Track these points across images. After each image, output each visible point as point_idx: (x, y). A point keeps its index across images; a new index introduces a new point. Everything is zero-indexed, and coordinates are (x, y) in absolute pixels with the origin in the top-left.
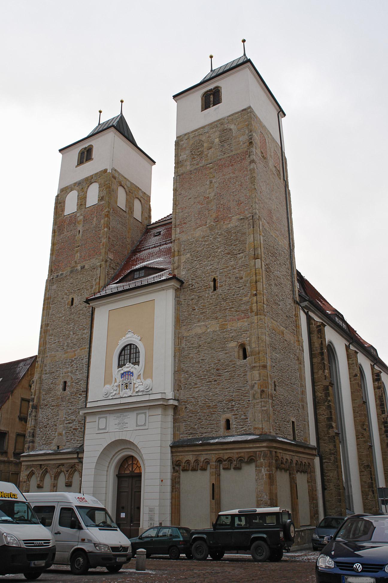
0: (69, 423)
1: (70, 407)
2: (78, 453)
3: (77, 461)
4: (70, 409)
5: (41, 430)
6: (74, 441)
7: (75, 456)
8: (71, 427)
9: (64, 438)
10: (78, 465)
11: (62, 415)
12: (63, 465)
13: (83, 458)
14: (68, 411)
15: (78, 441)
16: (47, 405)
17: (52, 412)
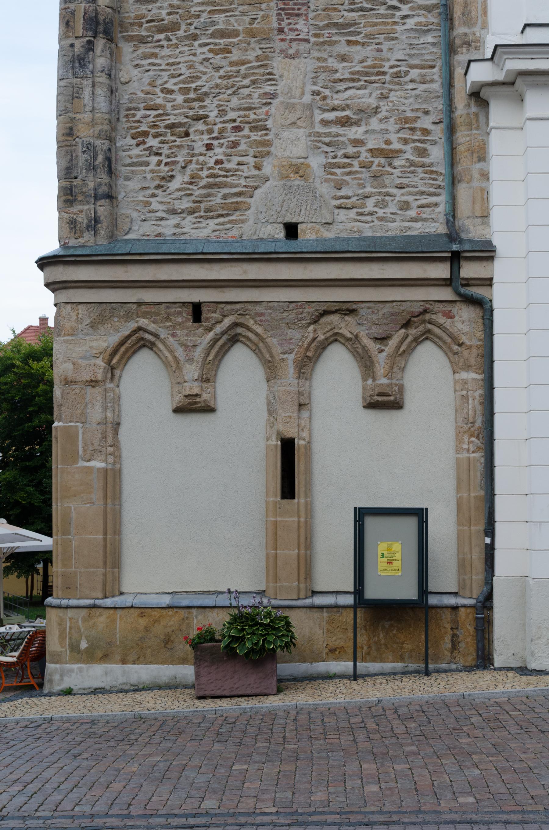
0: (345, 122)
1: (342, 48)
2: (456, 258)
3: (446, 294)
4: (343, 58)
5: (152, 142)
6: (383, 204)
7: (441, 271)
8: (357, 143)
9: (325, 190)
10: (449, 315)
11: (295, 75)
12: (348, 310)
13: (488, 282)
14: (332, 63)
15: (405, 206)
16: (174, 27)
17: (218, 60)
